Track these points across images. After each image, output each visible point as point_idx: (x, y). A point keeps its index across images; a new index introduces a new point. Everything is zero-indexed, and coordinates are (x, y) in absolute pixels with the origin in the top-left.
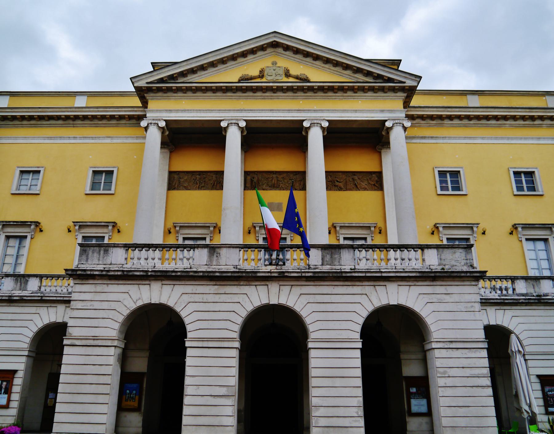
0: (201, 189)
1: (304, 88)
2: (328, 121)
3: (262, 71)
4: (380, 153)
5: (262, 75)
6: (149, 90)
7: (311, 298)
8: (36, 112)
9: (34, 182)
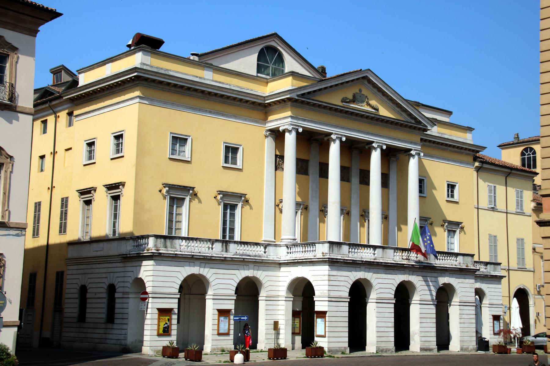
2: (386, 144)
3: (354, 96)
8: (187, 83)
9: (182, 149)
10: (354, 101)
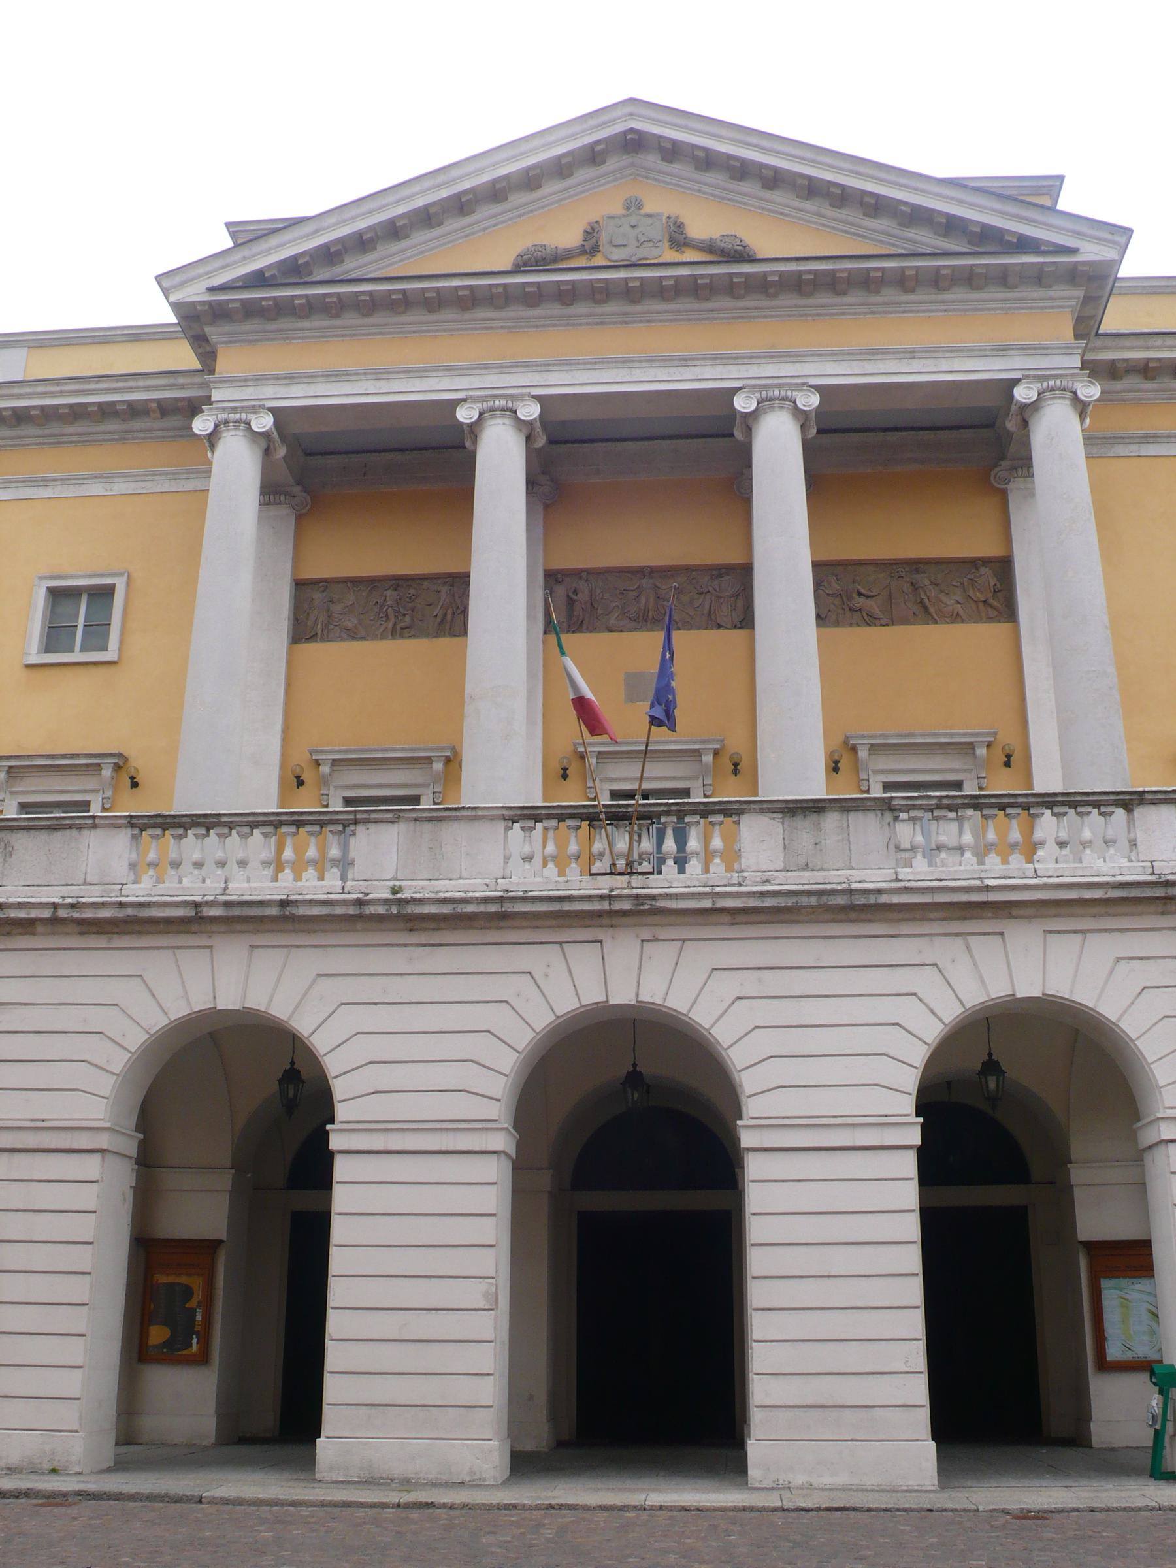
0: (402, 636)
1: (730, 284)
2: (818, 388)
3: (591, 232)
4: (1004, 494)
5: (591, 244)
6: (217, 313)
7: (749, 983)
10: (594, 250)
